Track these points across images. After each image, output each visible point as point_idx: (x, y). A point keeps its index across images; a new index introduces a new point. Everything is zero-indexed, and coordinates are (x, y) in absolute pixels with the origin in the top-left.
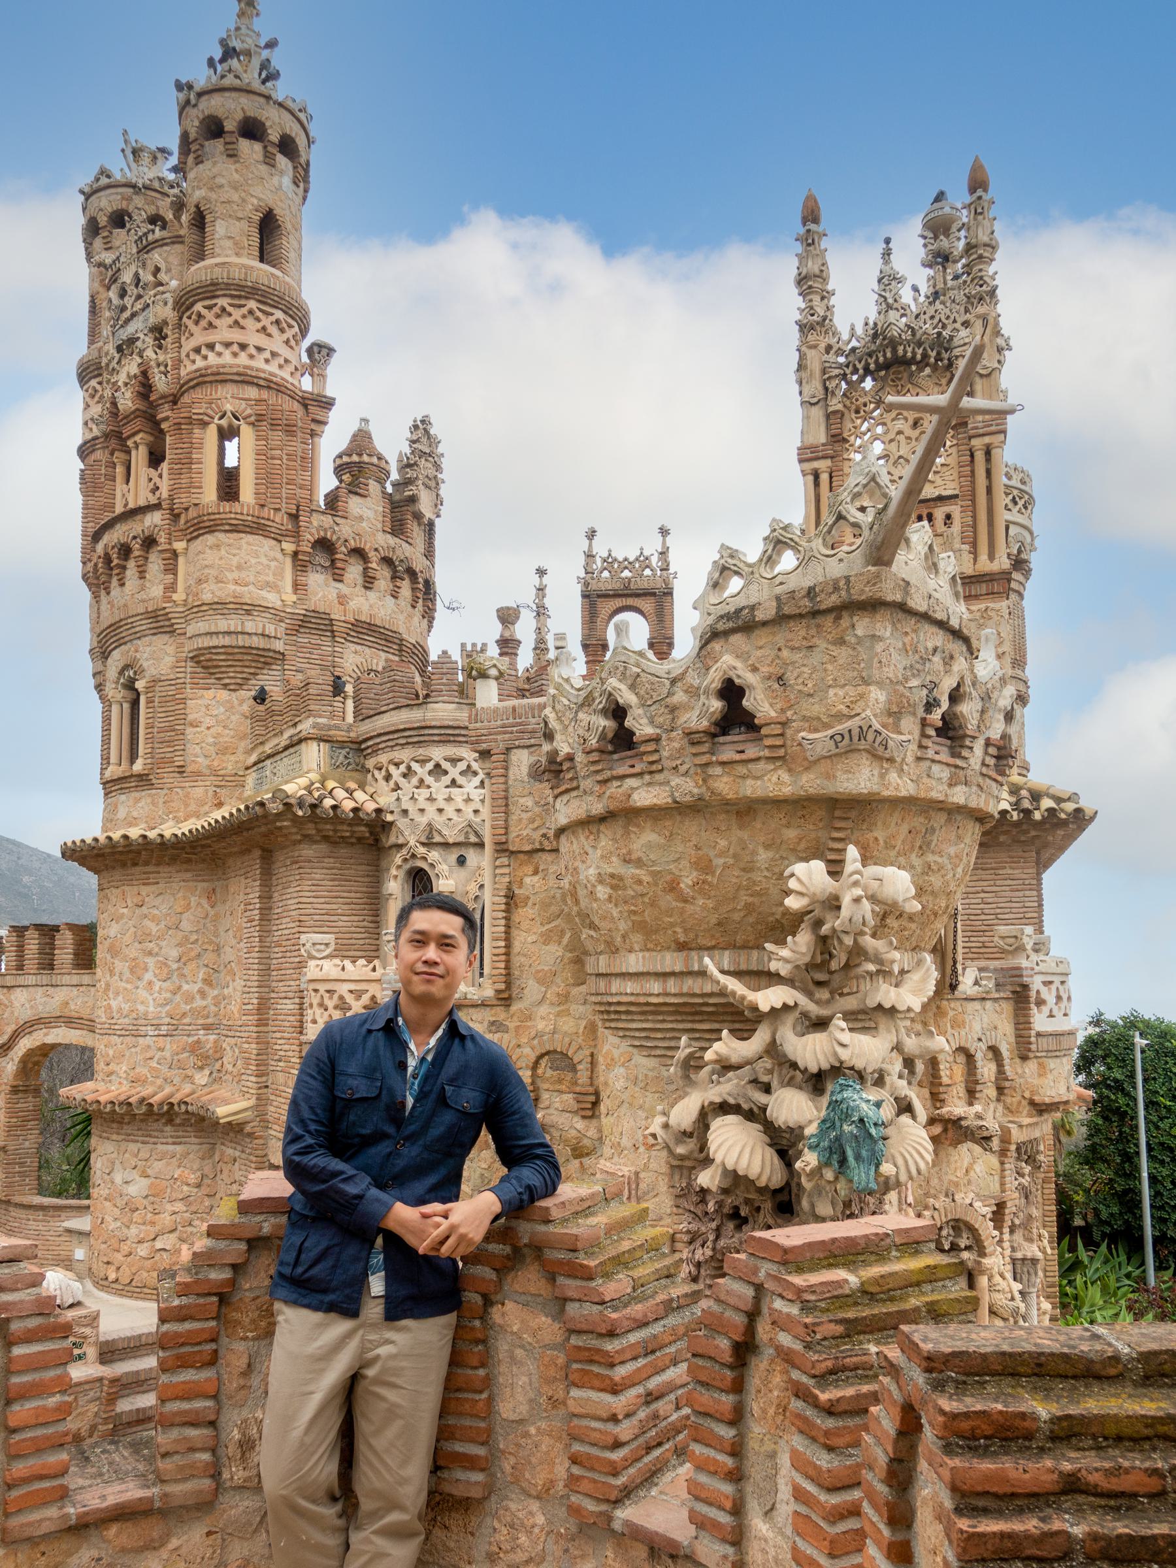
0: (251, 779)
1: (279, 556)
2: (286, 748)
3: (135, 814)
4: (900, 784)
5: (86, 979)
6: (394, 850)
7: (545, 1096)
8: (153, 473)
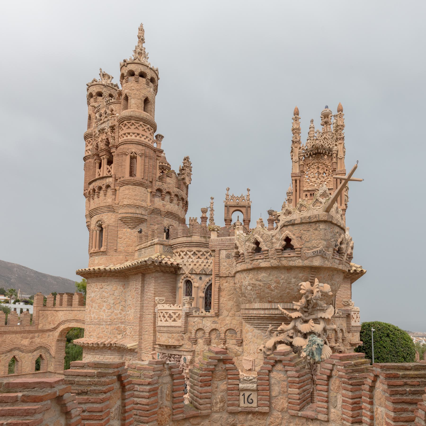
0: (137, 254)
2: (149, 246)
3: (101, 262)
4: (328, 264)
5: (82, 309)
6: (181, 275)
7: (228, 340)
8: (108, 166)
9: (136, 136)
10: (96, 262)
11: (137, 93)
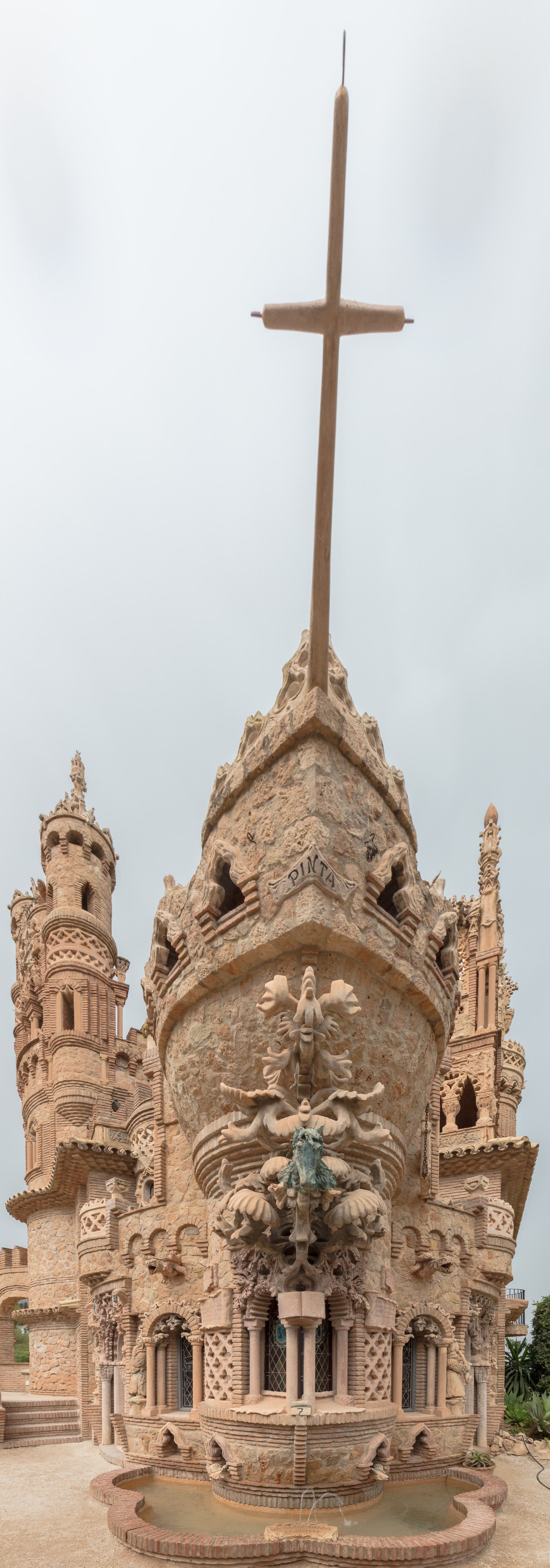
1: (99, 1060)
9: (70, 957)
11: (67, 875)
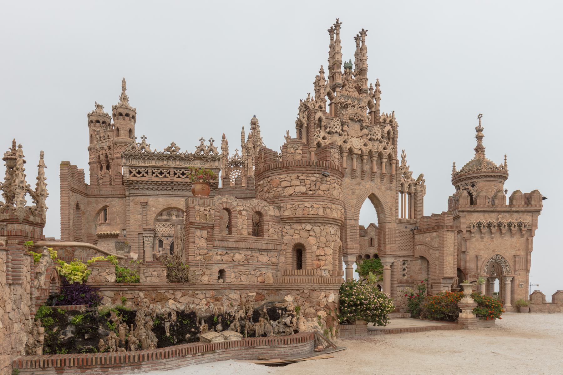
10: (103, 229)
